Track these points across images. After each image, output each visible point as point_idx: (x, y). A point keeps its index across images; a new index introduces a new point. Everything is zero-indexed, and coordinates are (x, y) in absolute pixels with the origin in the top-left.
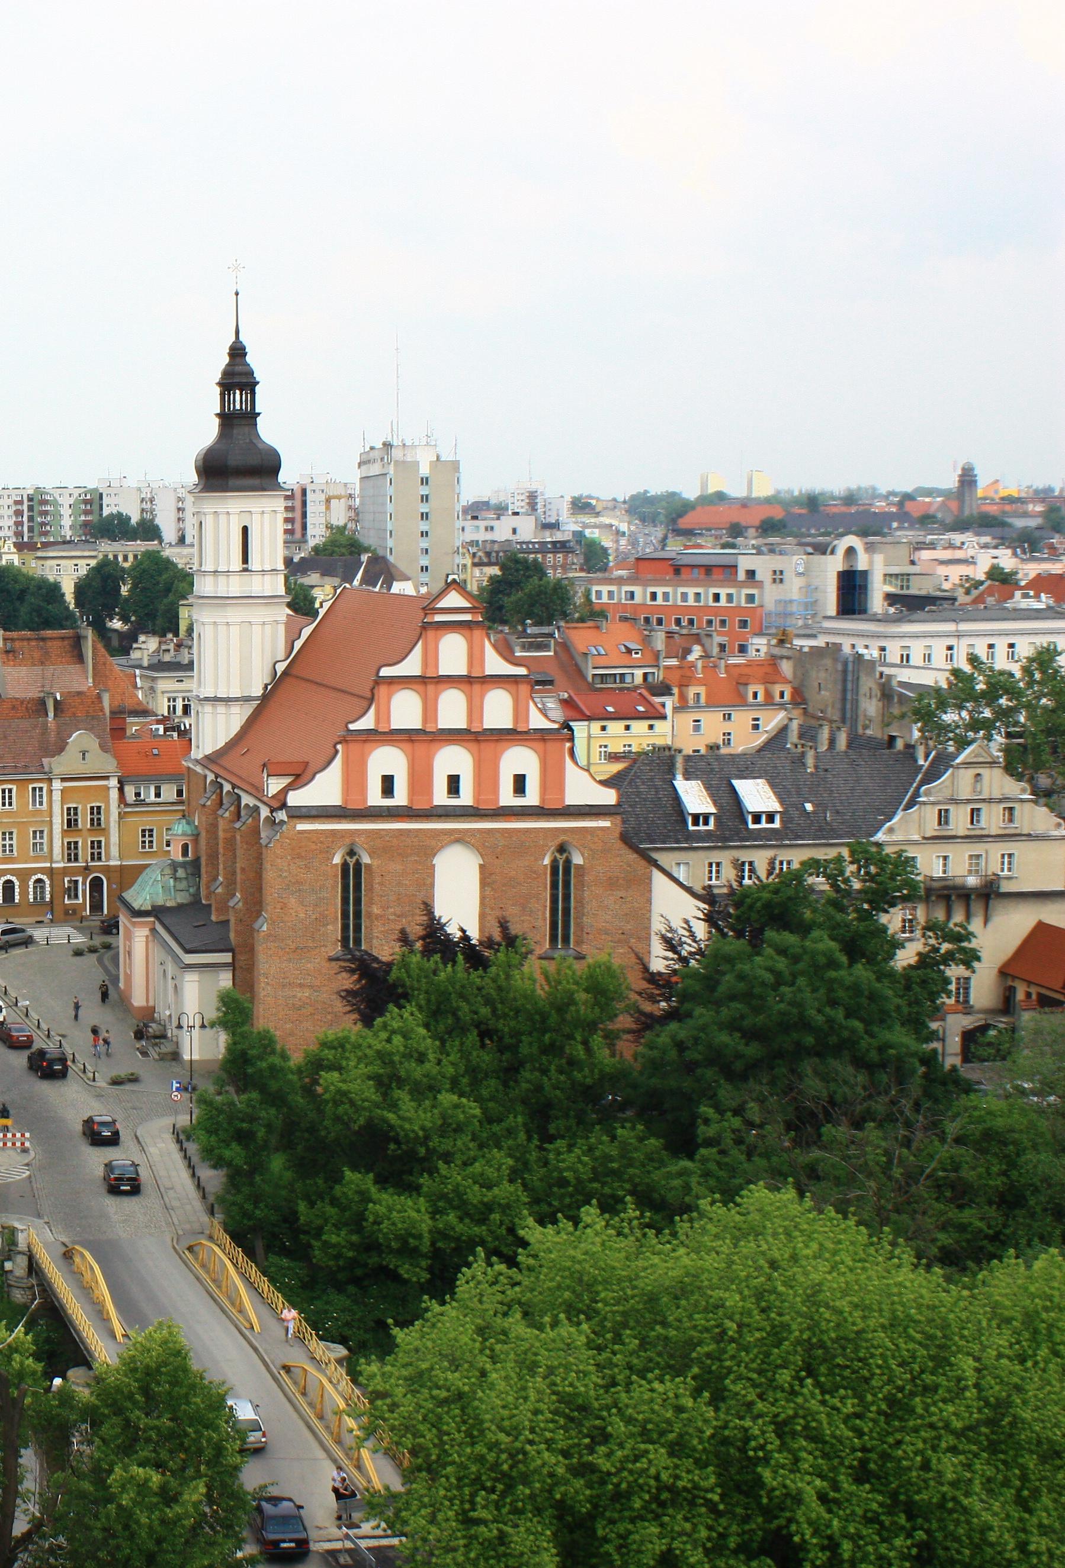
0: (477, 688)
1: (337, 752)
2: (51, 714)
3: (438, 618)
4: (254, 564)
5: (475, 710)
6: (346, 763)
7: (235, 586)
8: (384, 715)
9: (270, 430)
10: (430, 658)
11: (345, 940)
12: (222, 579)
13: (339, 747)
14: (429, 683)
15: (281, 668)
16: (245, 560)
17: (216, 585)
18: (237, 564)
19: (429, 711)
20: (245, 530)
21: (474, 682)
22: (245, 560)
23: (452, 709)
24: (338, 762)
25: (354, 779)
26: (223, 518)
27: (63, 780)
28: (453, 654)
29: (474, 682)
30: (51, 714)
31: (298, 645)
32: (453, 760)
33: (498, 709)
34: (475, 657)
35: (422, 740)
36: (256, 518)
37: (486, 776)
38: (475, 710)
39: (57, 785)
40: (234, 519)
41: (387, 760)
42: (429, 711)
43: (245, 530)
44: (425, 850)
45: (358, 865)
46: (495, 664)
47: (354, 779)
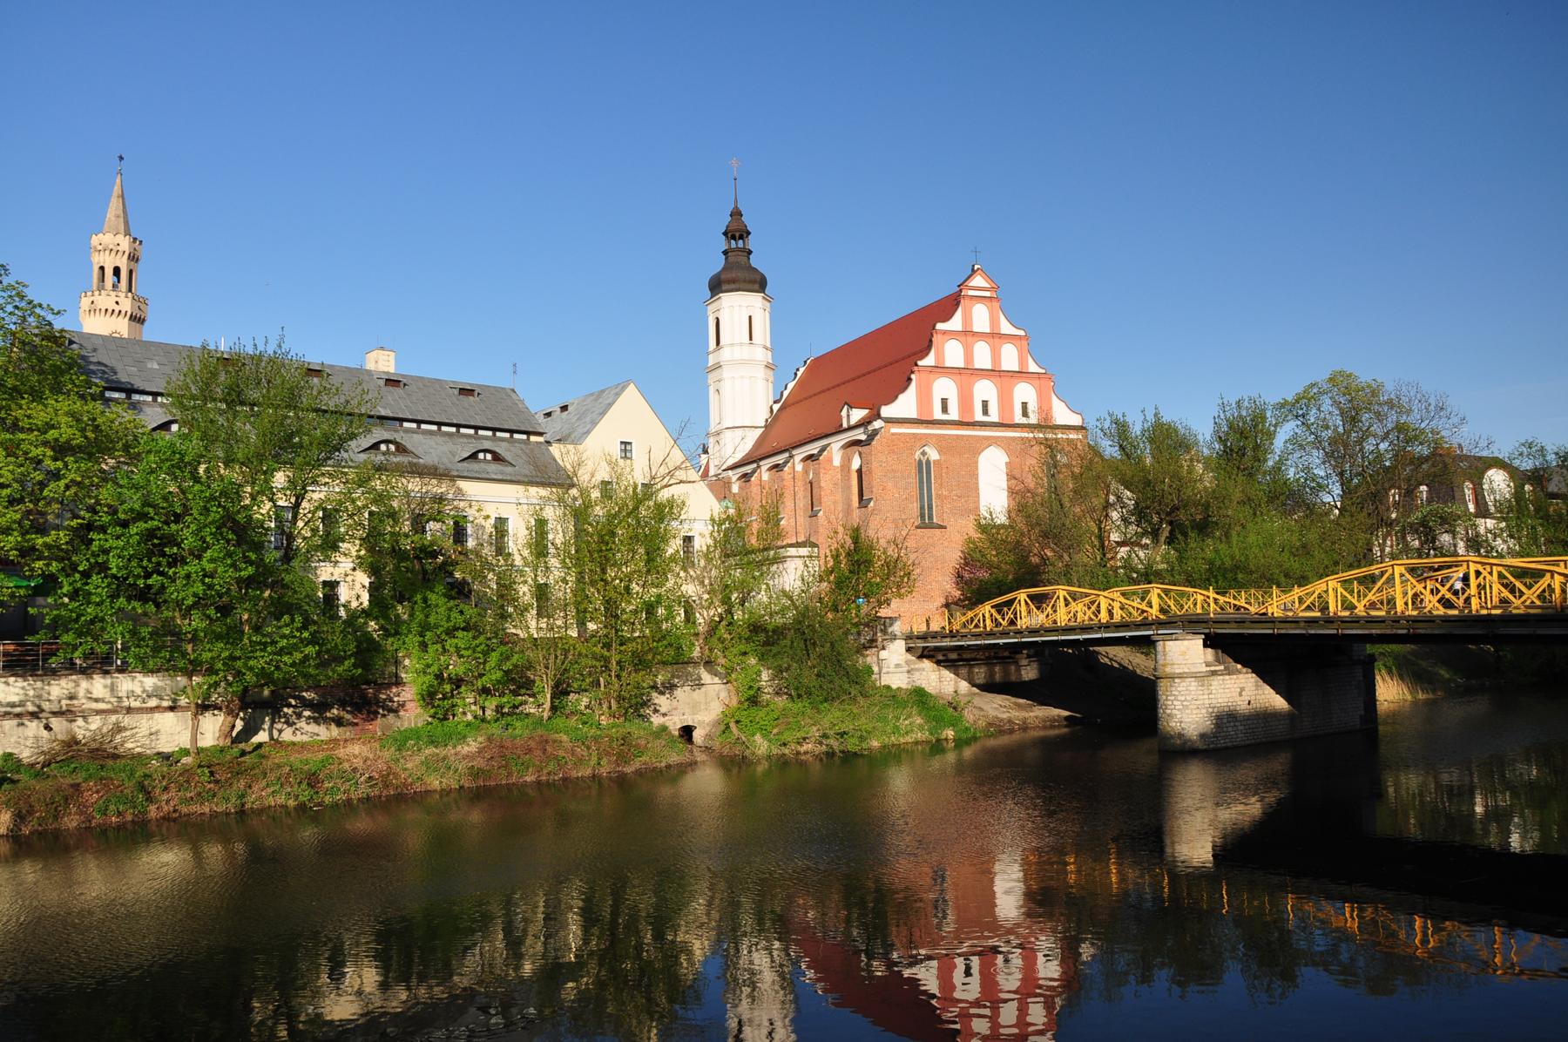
1: (910, 379)
3: (971, 293)
5: (996, 356)
6: (919, 387)
8: (940, 356)
9: (755, 261)
10: (967, 319)
11: (922, 516)
12: (737, 348)
14: (967, 335)
15: (776, 407)
19: (969, 355)
21: (995, 337)
23: (982, 356)
24: (913, 387)
25: (924, 398)
28: (980, 317)
29: (995, 337)
31: (786, 394)
32: (985, 390)
33: (1010, 358)
34: (994, 321)
35: (966, 374)
37: (1005, 399)
38: (996, 356)
41: (944, 388)
42: (969, 355)
44: (976, 447)
45: (928, 462)
46: (1006, 328)
47: (924, 398)
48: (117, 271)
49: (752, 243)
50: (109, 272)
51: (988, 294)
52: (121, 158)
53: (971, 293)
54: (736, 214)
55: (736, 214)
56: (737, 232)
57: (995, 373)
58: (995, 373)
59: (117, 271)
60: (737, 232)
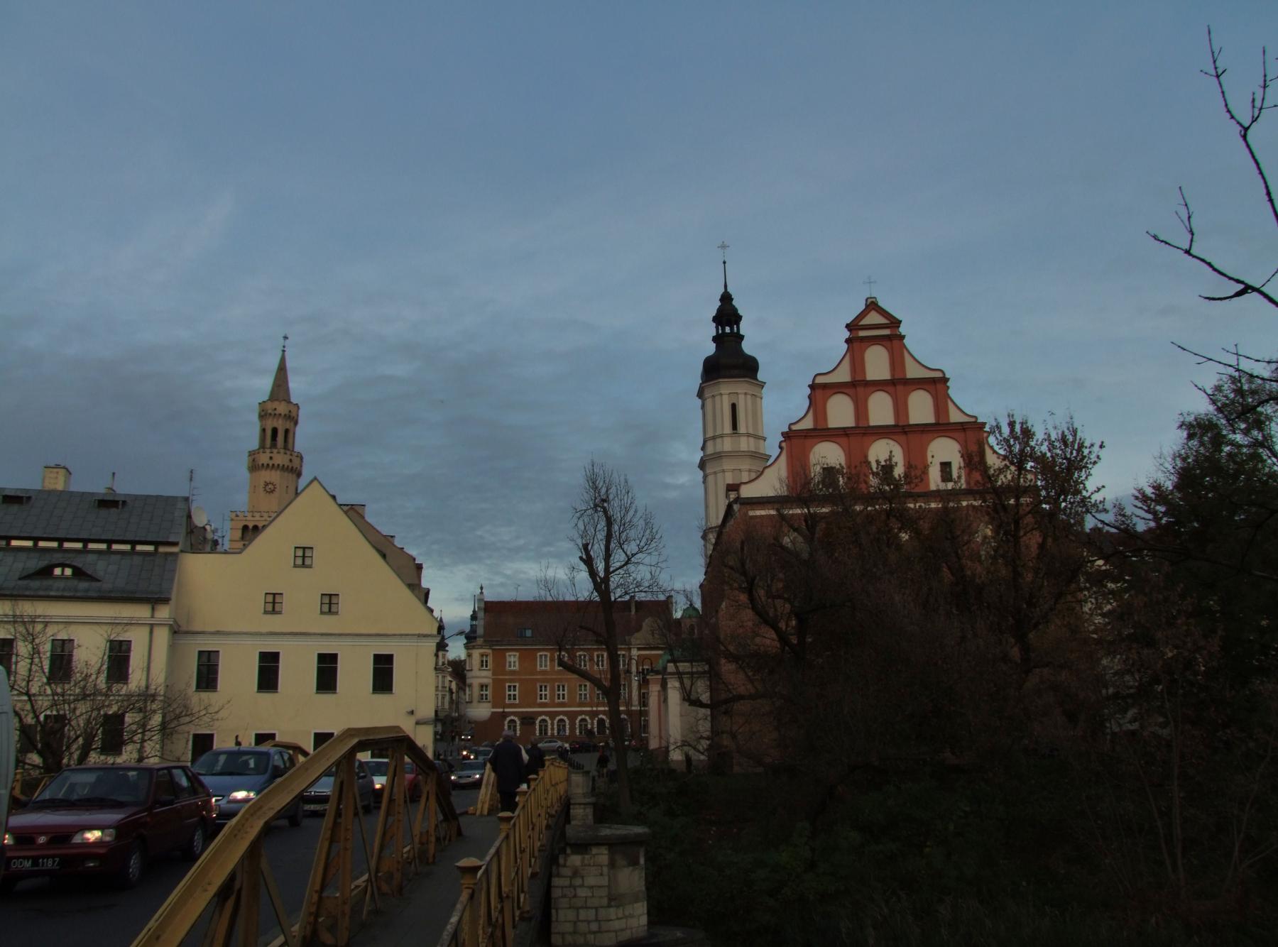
0: (900, 388)
2: (633, 612)
3: (862, 333)
4: (742, 429)
5: (900, 408)
7: (727, 445)
9: (748, 347)
12: (719, 441)
13: (784, 445)
14: (858, 387)
16: (735, 426)
17: (715, 445)
18: (728, 429)
19: (861, 410)
20: (734, 407)
22: (735, 426)
23: (881, 410)
26: (718, 398)
27: (639, 649)
30: (633, 612)
36: (741, 397)
38: (900, 408)
39: (635, 652)
40: (725, 398)
42: (861, 410)
43: (734, 407)
48: (275, 431)
49: (744, 328)
50: (269, 433)
51: (886, 332)
52: (286, 338)
53: (862, 333)
54: (726, 298)
55: (726, 298)
56: (727, 315)
57: (901, 430)
58: (901, 430)
59: (275, 431)
60: (727, 315)
